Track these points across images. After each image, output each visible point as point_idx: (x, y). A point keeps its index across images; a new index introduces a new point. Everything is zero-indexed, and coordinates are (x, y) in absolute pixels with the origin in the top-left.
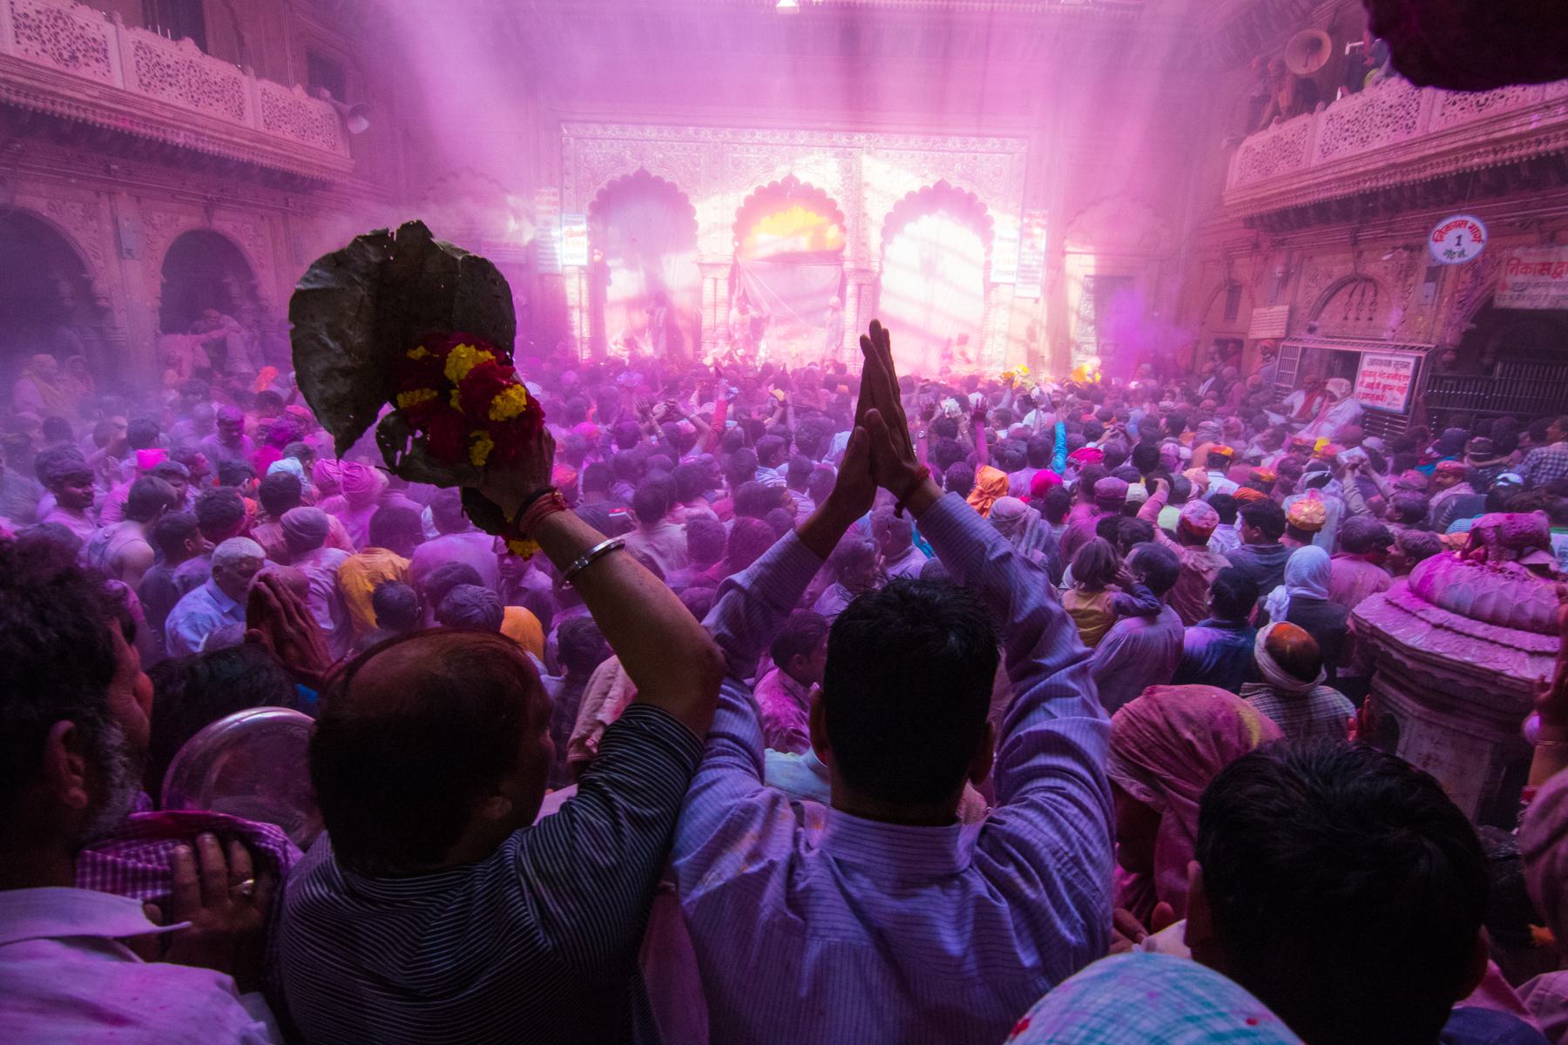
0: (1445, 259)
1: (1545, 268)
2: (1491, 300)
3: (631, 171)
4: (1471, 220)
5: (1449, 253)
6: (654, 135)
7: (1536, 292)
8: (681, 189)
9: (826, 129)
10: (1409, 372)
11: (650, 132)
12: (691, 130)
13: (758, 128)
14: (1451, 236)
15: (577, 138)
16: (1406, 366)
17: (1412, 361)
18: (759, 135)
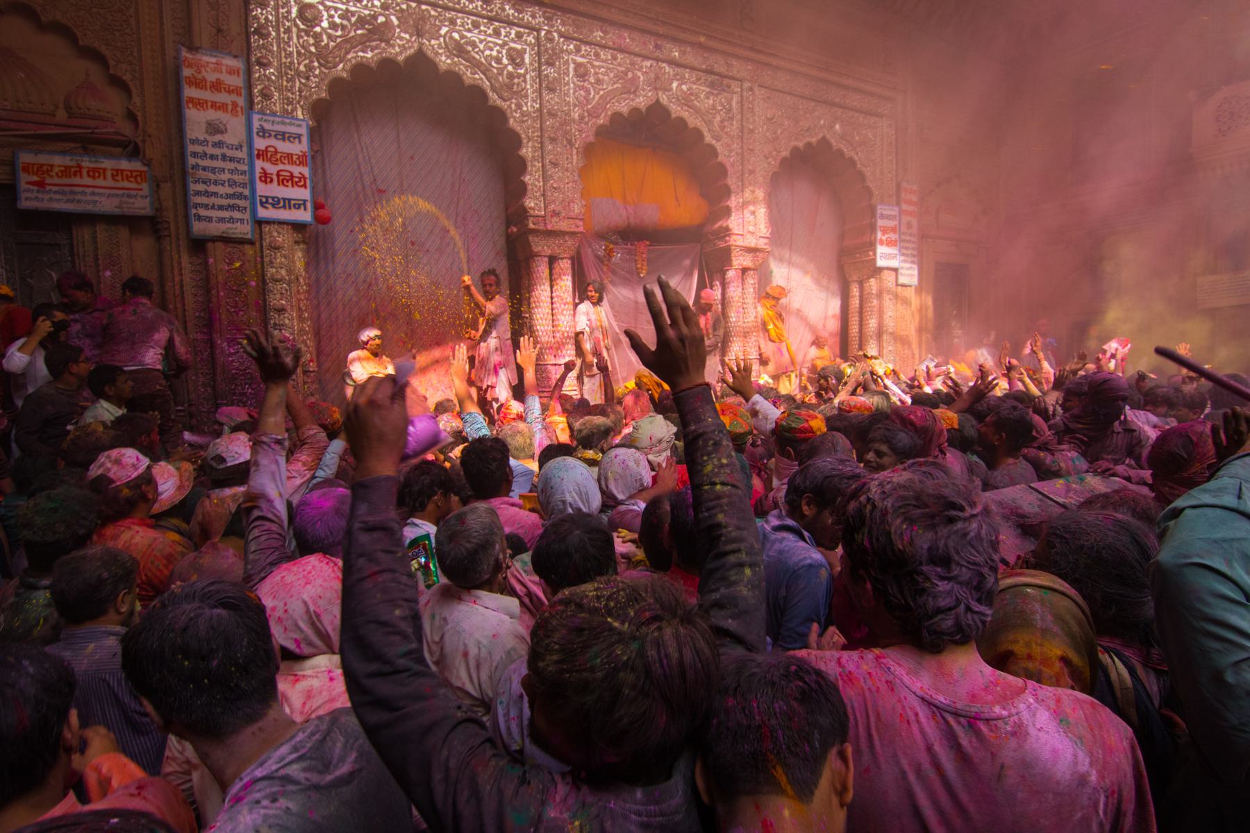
3: (402, 45)
9: (700, 46)
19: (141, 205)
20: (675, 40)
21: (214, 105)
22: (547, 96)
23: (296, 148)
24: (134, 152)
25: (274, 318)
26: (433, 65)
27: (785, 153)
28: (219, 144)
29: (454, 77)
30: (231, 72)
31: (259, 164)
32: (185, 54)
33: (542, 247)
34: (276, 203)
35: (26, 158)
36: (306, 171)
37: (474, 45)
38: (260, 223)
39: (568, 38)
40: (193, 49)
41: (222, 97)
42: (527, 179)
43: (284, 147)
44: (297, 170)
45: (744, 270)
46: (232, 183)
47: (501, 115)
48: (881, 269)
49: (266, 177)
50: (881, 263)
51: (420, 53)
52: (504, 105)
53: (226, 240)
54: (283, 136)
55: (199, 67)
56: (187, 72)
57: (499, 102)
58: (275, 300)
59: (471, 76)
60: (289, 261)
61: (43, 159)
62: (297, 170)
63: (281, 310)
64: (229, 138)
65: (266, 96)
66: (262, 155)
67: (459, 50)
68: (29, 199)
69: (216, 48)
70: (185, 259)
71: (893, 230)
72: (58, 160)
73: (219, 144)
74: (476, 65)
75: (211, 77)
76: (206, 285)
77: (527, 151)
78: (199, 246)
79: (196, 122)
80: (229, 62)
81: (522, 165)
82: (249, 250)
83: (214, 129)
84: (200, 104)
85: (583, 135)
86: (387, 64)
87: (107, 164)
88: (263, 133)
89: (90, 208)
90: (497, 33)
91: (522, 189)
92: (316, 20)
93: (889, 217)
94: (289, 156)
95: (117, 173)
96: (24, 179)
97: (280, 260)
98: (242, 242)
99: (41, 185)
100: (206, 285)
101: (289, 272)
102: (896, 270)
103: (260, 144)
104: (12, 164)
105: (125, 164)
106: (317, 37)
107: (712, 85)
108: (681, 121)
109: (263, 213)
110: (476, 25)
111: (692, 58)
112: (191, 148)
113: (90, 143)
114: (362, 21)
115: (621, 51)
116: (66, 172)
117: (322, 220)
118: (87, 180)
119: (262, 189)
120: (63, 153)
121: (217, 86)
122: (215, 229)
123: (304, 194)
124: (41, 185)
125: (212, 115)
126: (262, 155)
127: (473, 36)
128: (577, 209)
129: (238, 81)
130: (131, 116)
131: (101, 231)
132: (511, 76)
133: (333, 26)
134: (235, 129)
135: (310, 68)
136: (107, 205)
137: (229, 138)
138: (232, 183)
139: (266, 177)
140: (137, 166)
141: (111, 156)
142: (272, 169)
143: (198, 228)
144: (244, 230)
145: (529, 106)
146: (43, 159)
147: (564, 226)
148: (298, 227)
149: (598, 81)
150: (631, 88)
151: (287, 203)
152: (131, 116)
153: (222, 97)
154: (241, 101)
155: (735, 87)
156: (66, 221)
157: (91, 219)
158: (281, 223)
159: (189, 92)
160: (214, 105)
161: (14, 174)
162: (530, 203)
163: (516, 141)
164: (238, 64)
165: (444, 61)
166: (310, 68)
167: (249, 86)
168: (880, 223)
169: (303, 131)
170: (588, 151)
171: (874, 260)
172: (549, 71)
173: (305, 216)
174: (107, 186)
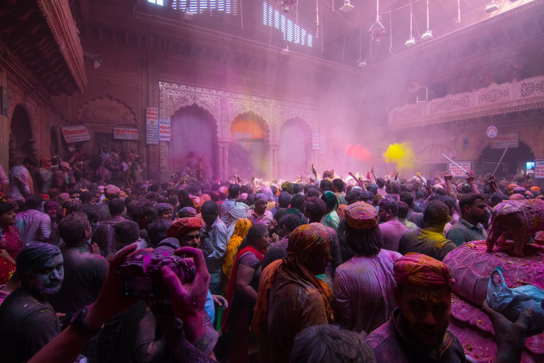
0: (490, 137)
1: (505, 139)
2: (490, 145)
3: (190, 103)
4: (494, 127)
5: (491, 135)
6: (200, 91)
7: (504, 144)
8: (211, 112)
9: (262, 97)
10: (470, 166)
11: (198, 90)
12: (215, 91)
13: (239, 93)
14: (491, 130)
15: (166, 88)
16: (468, 165)
17: (470, 164)
18: (239, 96)
19: (136, 138)
20: (255, 96)
21: (153, 118)
22: (223, 111)
23: (168, 126)
24: (135, 127)
25: (161, 161)
26: (197, 106)
27: (285, 121)
28: (153, 126)
29: (202, 109)
30: (156, 111)
31: (160, 129)
32: (147, 108)
33: (221, 145)
34: (163, 137)
35: (116, 129)
36: (169, 130)
37: (206, 101)
38: (160, 141)
39: (229, 97)
40: (149, 107)
41: (154, 116)
42: (218, 130)
43: (165, 125)
44: (168, 130)
45: (274, 150)
46: (155, 133)
47: (212, 116)
48: (314, 150)
49: (161, 132)
50: (313, 148)
51: (195, 103)
52: (213, 114)
53: (153, 145)
54: (165, 123)
55: (150, 110)
56: (148, 112)
57: (212, 113)
58: (162, 157)
59: (205, 108)
60: (165, 149)
61: (118, 129)
62: (168, 130)
63: (163, 160)
64: (155, 124)
65: (162, 115)
66: (161, 127)
67: (203, 102)
68: (116, 137)
69: (153, 106)
70: (144, 149)
71: (318, 140)
72: (121, 129)
73: (153, 126)
74: (207, 105)
75: (152, 112)
76: (148, 154)
77: (218, 124)
78: (147, 146)
79: (149, 121)
80: (156, 109)
81: (216, 127)
82: (157, 147)
83: (152, 122)
84: (149, 118)
85: (232, 119)
86: (188, 107)
87: (131, 129)
88: (161, 123)
89: (126, 138)
90: (212, 98)
91: (217, 132)
92: (173, 98)
93: (316, 136)
94: (166, 127)
95: (132, 131)
96: (115, 132)
97: (163, 149)
98: (156, 145)
99: (118, 134)
100: (148, 154)
101: (165, 151)
102: (318, 150)
103: (161, 125)
104: (113, 129)
105: (134, 130)
106: (173, 102)
107: (265, 105)
108: (257, 115)
109: (160, 139)
110: (207, 96)
111: (259, 99)
112: (147, 127)
113: (128, 125)
114: (182, 98)
115: (241, 99)
116: (123, 131)
117: (172, 140)
118: (126, 133)
119: (161, 134)
120: (122, 127)
121: (153, 114)
122: (151, 143)
123: (169, 135)
124: (118, 134)
125: (152, 120)
126: (161, 127)
127: (206, 99)
128: (230, 136)
129: (157, 113)
130: (135, 119)
131: (128, 143)
132: (215, 107)
133: (176, 99)
134: (156, 122)
135: (171, 108)
136: (130, 138)
137: (155, 124)
138: (155, 133)
139: (161, 132)
140: (136, 130)
141: (131, 128)
142: (163, 130)
143: (148, 142)
144: (156, 143)
145: (219, 113)
146: (118, 129)
147: (226, 140)
148: (167, 142)
149: (236, 107)
150: (244, 108)
151: (165, 137)
152: (135, 119)
153: (154, 116)
154: (157, 117)
155: (272, 105)
156: (121, 141)
157: (127, 140)
158: (164, 141)
159: (148, 115)
160: (153, 118)
161: (113, 132)
162: (218, 135)
163: (215, 121)
164: (157, 109)
165: (200, 105)
166: (171, 108)
167: (159, 113)
168: (313, 138)
169: (169, 122)
170: (233, 123)
171: (312, 148)
172: (224, 105)
173: (169, 140)
174: (130, 134)
